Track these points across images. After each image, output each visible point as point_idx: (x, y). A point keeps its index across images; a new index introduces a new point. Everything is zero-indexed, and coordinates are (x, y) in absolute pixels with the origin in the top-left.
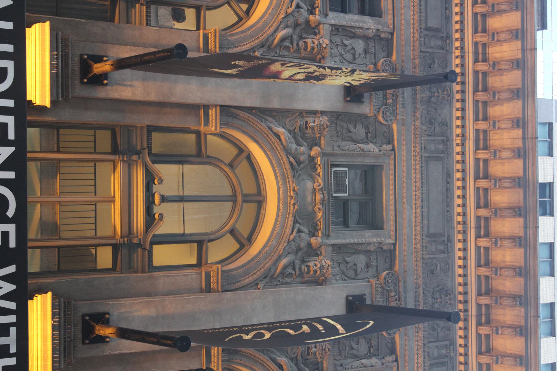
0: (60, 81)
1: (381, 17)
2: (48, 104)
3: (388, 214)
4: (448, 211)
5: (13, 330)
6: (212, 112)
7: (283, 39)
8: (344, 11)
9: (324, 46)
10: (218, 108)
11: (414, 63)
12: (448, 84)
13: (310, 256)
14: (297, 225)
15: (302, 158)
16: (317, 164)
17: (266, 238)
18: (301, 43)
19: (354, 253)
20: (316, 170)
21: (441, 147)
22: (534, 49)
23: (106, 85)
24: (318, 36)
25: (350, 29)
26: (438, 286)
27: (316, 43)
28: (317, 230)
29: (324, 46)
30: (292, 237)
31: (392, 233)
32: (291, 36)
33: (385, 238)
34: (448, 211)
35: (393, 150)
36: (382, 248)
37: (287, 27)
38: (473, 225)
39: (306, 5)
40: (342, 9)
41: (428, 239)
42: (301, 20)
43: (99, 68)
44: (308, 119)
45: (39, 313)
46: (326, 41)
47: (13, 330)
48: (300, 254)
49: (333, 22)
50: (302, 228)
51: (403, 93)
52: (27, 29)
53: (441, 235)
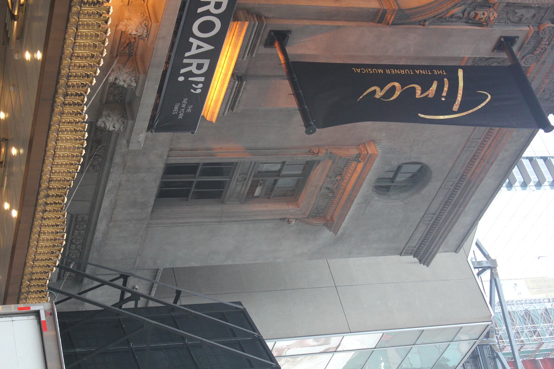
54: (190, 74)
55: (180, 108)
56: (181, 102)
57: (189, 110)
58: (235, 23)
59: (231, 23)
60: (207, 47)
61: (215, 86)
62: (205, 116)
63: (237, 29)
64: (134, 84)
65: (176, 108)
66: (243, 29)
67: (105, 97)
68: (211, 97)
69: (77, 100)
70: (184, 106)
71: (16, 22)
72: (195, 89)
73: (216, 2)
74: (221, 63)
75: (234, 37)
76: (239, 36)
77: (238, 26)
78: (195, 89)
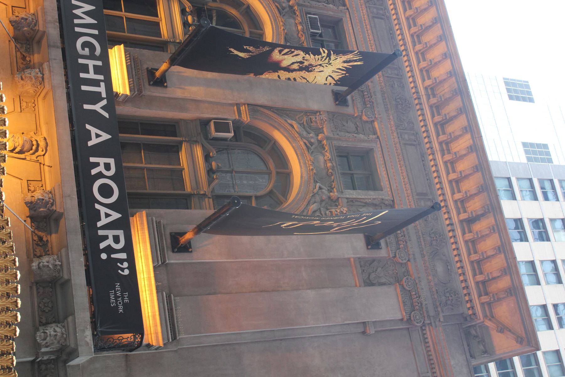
0: (166, 308)
1: (382, 190)
2: (161, 344)
3: (384, 183)
4: (427, 180)
5: (102, 84)
6: (243, 108)
7: (315, 212)
8: (354, 188)
9: (345, 212)
10: (246, 106)
11: (394, 141)
12: (436, 212)
13: (331, 206)
14: (318, 185)
15: (312, 140)
16: (323, 145)
17: (296, 193)
18: (327, 212)
19: (364, 206)
20: (324, 148)
21: (413, 137)
22: (480, 137)
23: (166, 87)
24: (339, 207)
25: (362, 200)
26: (432, 230)
27: (339, 211)
28: (333, 189)
29: (345, 212)
30: (315, 191)
31: (390, 193)
32: (320, 209)
33: (385, 195)
34: (427, 180)
35: (378, 137)
36: (384, 204)
37: (315, 202)
38: (453, 207)
39: (325, 186)
40: (353, 187)
41: (417, 197)
42: (324, 197)
43: (183, 240)
44: (311, 117)
46: (345, 210)
47: (102, 84)
48: (323, 204)
49: (348, 196)
50: (323, 187)
51: (407, 229)
52: (109, 50)
53: (425, 194)
54: (109, 250)
58: (134, 218)
59: (131, 218)
60: (116, 216)
63: (138, 223)
64: (58, 263)
66: (143, 220)
75: (139, 232)
77: (138, 219)
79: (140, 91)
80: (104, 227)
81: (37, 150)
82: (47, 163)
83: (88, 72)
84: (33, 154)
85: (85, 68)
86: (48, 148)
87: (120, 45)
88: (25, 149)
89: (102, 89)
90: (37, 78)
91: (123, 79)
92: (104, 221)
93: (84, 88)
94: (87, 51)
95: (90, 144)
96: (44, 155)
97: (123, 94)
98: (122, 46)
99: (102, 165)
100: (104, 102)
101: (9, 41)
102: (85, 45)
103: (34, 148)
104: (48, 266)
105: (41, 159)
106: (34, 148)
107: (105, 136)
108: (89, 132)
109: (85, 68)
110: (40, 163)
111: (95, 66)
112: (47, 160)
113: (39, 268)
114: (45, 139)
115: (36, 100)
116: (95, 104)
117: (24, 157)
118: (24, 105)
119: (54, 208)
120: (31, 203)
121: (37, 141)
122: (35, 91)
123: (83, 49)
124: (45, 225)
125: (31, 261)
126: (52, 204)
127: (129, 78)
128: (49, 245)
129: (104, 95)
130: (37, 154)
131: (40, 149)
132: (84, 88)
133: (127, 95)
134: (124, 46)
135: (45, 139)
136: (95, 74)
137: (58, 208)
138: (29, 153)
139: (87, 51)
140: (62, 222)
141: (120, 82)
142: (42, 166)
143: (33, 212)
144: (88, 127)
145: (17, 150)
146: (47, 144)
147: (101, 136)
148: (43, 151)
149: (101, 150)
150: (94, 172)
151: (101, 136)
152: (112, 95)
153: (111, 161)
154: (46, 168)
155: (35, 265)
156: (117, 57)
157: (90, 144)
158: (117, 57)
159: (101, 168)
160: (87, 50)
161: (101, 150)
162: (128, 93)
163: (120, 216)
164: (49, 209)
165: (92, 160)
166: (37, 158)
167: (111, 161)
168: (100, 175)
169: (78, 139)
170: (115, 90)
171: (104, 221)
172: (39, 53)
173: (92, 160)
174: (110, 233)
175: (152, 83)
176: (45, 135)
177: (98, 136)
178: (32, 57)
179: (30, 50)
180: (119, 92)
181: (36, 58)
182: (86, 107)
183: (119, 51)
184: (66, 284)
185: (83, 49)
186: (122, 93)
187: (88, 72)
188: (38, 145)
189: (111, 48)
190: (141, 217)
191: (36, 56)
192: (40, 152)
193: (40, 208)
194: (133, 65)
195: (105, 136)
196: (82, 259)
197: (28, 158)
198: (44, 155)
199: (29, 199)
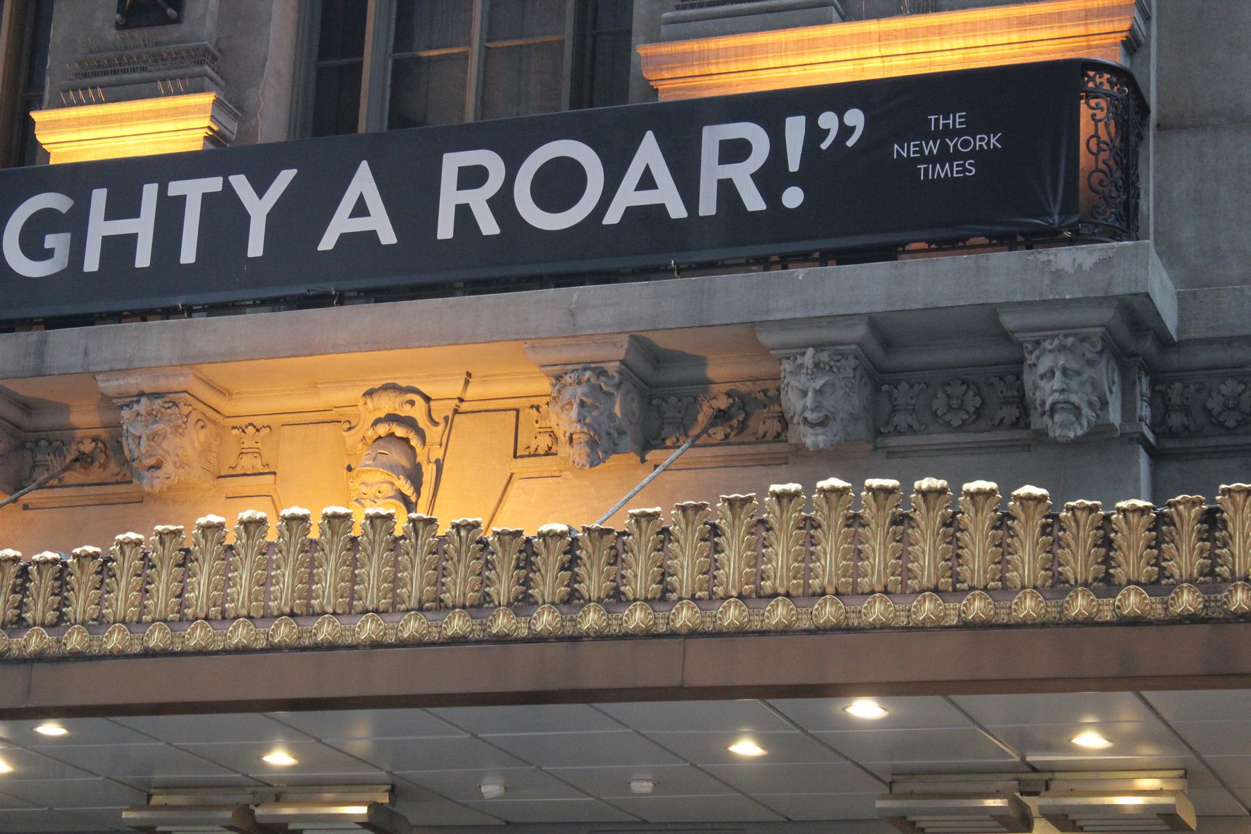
5: (175, 188)
45: (127, 131)
47: (175, 188)
52: (52, 162)
54: (772, 178)
55: (944, 156)
56: (910, 165)
57: (957, 120)
58: (661, 86)
59: (662, 98)
60: (649, 153)
61: (958, 55)
62: (1120, 37)
63: (680, 73)
64: (808, 358)
65: (941, 171)
66: (671, 55)
67: (1002, 435)
68: (1017, 49)
69: (41, 585)
70: (932, 147)
71: (124, 815)
72: (846, 131)
73: (138, 215)
74: (846, 73)
75: (713, 70)
76: (703, 58)
77: (666, 75)
78: (846, 131)
79: (203, 55)
80: (689, 193)
81: (410, 423)
82: (455, 389)
83: (132, 239)
84: (421, 434)
85: (119, 248)
86: (403, 383)
87: (33, 123)
88: (404, 462)
89: (193, 191)
90: (153, 417)
91: (157, 115)
92: (668, 196)
93: (188, 255)
94: (57, 242)
95: (388, 236)
96: (427, 399)
97: (213, 118)
98: (36, 116)
99: (467, 196)
100: (241, 184)
101: (26, 507)
102: (33, 246)
103: (400, 432)
104: (819, 392)
105: (441, 410)
106: (400, 432)
107: (363, 183)
108: (344, 238)
109: (119, 248)
110: (456, 412)
111: (112, 213)
112: (445, 389)
113: (822, 423)
114: (370, 393)
115: (236, 422)
116: (246, 218)
117: (434, 467)
118: (248, 463)
119: (612, 367)
120: (593, 444)
121: (377, 422)
122: (202, 423)
123: (48, 254)
124: (673, 400)
125: (799, 451)
126: (602, 373)
127: (155, 95)
128: (743, 388)
129: (214, 184)
130: (423, 422)
131: (407, 411)
132: (188, 255)
133: (217, 103)
134: (40, 107)
135: (370, 393)
136: (136, 214)
137: (614, 354)
138: (419, 449)
139: (57, 242)
140: (663, 341)
141: (172, 124)
142: (464, 407)
143: (627, 440)
144: (328, 242)
145: (408, 490)
146: (386, 388)
147: (361, 197)
148: (412, 403)
149: (411, 198)
150: (489, 226)
151: (361, 197)
152: (215, 157)
153: (452, 163)
154: (472, 392)
155: (812, 439)
156: (75, 134)
157: (388, 236)
158: (75, 134)
159: (478, 200)
160: (50, 241)
161: (411, 198)
162: (207, 99)
163: (649, 137)
164: (618, 386)
165: (445, 229)
166: (436, 424)
167: (452, 163)
168: (502, 204)
169: (371, 278)
170: (197, 146)
171: (668, 196)
172: (64, 409)
173: (445, 229)
174: (711, 171)
175: (170, 11)
176: (355, 394)
177: (361, 209)
178: (79, 434)
179: (58, 440)
180: (202, 134)
181: (85, 418)
182: (256, 247)
183: (55, 126)
184: (886, 333)
185: (48, 254)
186: (207, 122)
187: (132, 239)
188: (391, 418)
189: (47, 155)
190: (660, 62)
191: (76, 418)
192: (418, 412)
193: (612, 416)
194: (106, 79)
195: (363, 183)
196: (799, 273)
197: (437, 453)
198: (427, 399)
199: (578, 453)
